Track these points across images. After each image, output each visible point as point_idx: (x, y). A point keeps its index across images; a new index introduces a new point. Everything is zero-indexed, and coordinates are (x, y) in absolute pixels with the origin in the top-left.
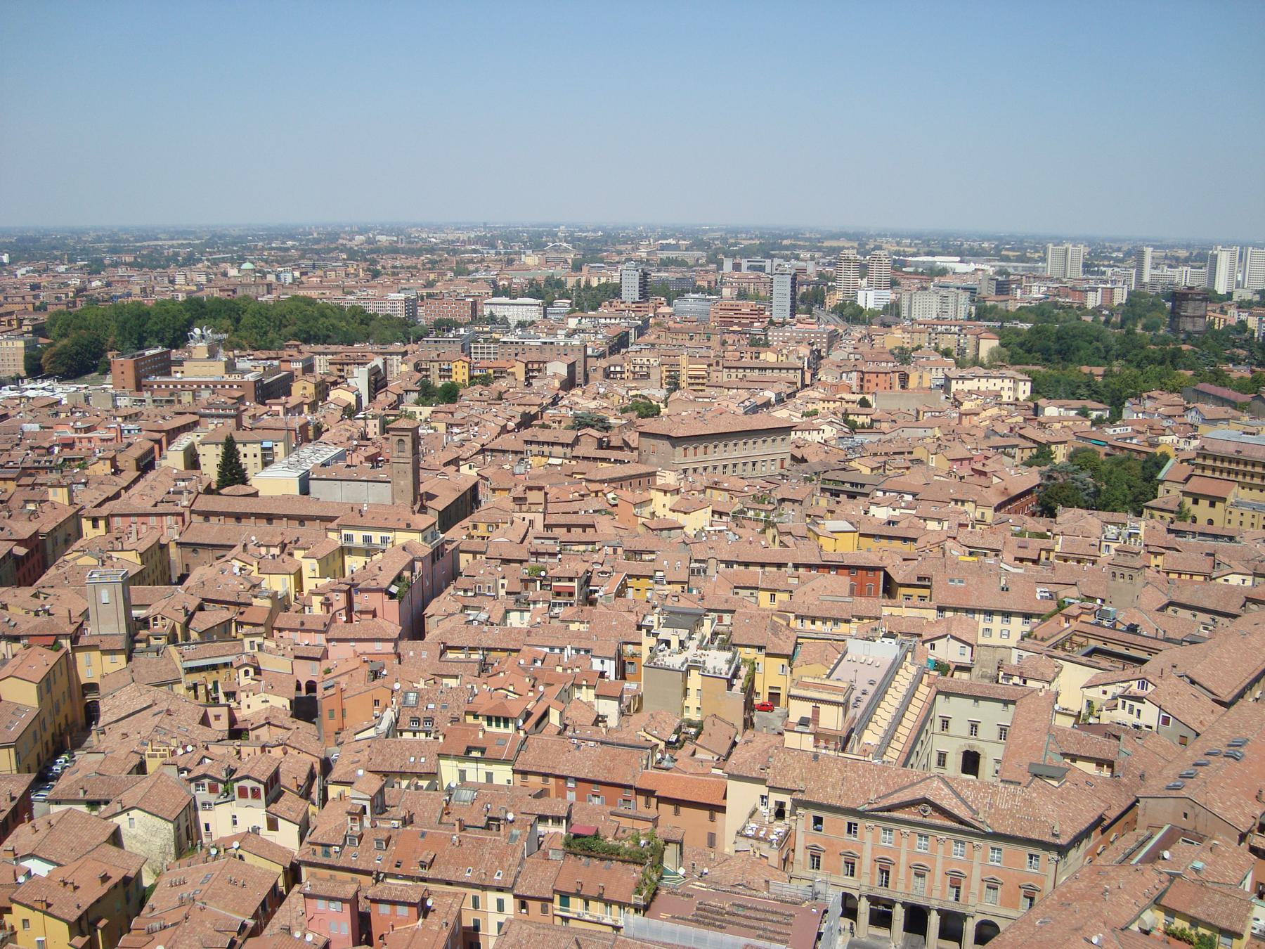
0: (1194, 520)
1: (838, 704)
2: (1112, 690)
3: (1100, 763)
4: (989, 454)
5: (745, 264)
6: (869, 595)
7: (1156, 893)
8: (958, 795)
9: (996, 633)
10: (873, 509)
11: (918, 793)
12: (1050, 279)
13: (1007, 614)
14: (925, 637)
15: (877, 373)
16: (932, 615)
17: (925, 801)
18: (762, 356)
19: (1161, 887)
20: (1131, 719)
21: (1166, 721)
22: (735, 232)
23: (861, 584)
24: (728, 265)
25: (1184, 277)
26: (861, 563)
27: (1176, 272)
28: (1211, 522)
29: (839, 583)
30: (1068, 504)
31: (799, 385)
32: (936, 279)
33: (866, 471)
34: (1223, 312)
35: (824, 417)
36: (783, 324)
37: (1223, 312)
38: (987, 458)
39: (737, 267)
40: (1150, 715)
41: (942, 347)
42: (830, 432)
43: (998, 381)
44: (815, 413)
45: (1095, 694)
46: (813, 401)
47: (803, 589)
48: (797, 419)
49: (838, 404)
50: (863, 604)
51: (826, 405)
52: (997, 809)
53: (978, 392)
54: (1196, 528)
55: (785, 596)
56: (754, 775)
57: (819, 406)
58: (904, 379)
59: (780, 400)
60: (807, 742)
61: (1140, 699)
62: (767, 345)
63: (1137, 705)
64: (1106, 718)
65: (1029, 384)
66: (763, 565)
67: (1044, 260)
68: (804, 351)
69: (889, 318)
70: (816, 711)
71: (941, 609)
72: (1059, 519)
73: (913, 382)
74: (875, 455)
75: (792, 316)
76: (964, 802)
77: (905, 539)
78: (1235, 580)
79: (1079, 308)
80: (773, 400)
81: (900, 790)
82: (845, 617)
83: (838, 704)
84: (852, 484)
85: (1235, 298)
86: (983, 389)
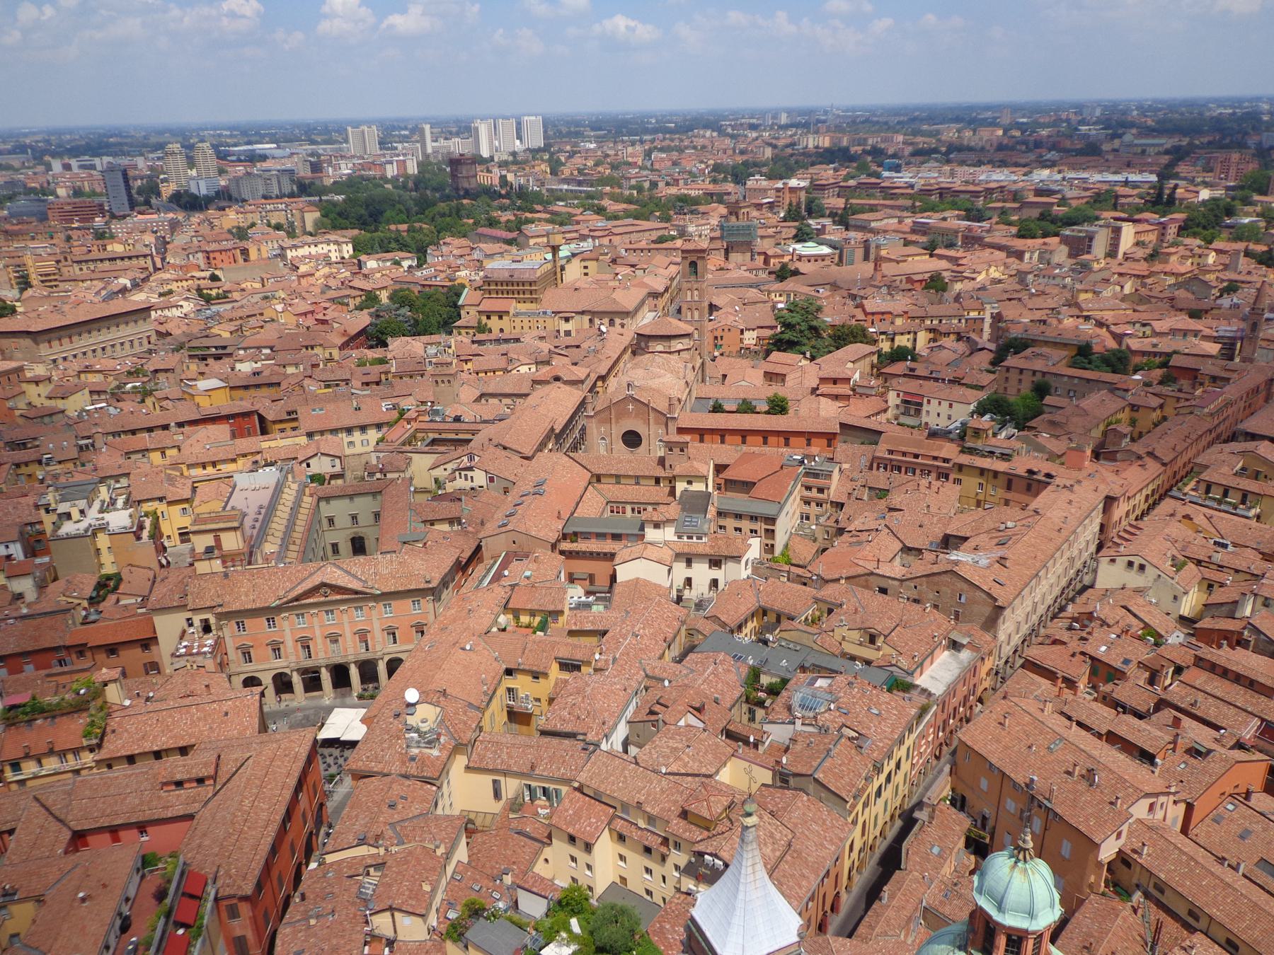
0: (490, 331)
1: (235, 529)
2: (450, 467)
3: (451, 521)
4: (327, 305)
5: (74, 163)
6: (249, 435)
7: (504, 601)
8: (348, 573)
9: (358, 444)
10: (238, 366)
11: (316, 580)
12: (353, 157)
13: (363, 428)
14: (301, 459)
15: (221, 251)
16: (303, 440)
17: (324, 585)
18: (109, 248)
19: (507, 596)
20: (468, 484)
21: (491, 480)
22: (59, 133)
23: (240, 428)
24: (57, 166)
25: (457, 146)
26: (236, 410)
27: (450, 143)
28: (502, 330)
29: (221, 431)
30: (394, 334)
31: (151, 269)
32: (258, 165)
33: (226, 335)
34: (489, 171)
35: (179, 295)
36: (124, 217)
37: (489, 171)
38: (325, 309)
39: (67, 167)
40: (480, 478)
41: (273, 222)
42: (188, 307)
43: (324, 246)
44: (170, 292)
45: (439, 472)
46: (167, 281)
47: (189, 441)
48: (154, 299)
49: (190, 282)
50: (245, 444)
51: (180, 284)
52: (381, 575)
53: (310, 256)
54: (492, 336)
55: (175, 451)
56: (175, 604)
57: (174, 286)
58: (245, 252)
59: (136, 285)
60: (217, 565)
61: (470, 469)
62: (112, 237)
63: (470, 474)
64: (450, 488)
65: (350, 246)
66: (150, 430)
67: (346, 141)
68: (149, 239)
69: (222, 204)
70: (217, 539)
71: (310, 435)
72: (390, 347)
73: (253, 255)
74: (231, 320)
75: (132, 209)
76: (355, 576)
77: (270, 385)
78: (524, 369)
79: (381, 178)
80: (129, 285)
81: (303, 581)
82: (230, 457)
83: (235, 529)
84: (216, 348)
85: (496, 159)
86: (313, 253)
